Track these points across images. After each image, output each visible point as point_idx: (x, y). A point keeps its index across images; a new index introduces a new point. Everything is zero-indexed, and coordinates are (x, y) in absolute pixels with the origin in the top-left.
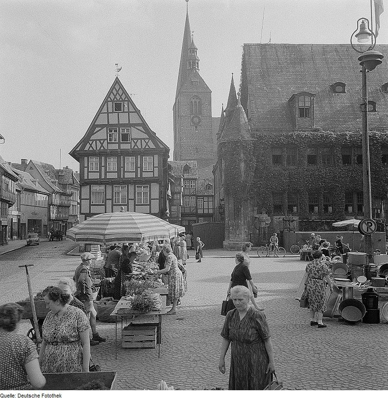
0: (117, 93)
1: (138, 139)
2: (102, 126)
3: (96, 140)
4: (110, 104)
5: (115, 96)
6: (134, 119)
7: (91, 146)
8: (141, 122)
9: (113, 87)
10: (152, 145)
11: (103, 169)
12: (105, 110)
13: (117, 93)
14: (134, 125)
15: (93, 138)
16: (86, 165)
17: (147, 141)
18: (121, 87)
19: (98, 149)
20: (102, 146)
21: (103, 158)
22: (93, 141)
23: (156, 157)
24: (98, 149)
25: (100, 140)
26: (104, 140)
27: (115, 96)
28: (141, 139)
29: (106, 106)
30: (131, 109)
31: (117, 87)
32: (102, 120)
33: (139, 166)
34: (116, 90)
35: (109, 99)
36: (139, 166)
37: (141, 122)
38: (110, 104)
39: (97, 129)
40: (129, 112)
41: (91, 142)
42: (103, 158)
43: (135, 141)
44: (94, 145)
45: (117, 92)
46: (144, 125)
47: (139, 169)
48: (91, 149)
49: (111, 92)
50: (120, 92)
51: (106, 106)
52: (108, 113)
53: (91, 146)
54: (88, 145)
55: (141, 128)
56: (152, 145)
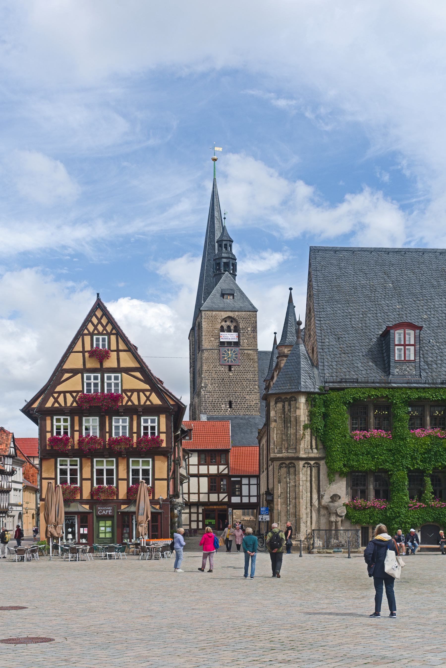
0: (100, 322)
1: (132, 391)
2: (75, 372)
3: (65, 392)
4: (87, 339)
5: (96, 327)
6: (127, 361)
7: (56, 401)
8: (138, 366)
9: (92, 313)
10: (155, 400)
11: (77, 435)
12: (78, 347)
13: (100, 322)
14: (127, 370)
15: (59, 388)
16: (48, 429)
17: (148, 394)
18: (106, 313)
19: (69, 405)
20: (74, 400)
21: (76, 419)
22: (59, 393)
23: (163, 419)
24: (69, 405)
25: (71, 392)
26: (77, 392)
27: (96, 327)
28: (138, 391)
29: (80, 343)
30: (122, 346)
31: (99, 313)
32: (75, 362)
33: (135, 430)
34: (97, 317)
35: (86, 332)
36: (135, 430)
37: (138, 366)
38: (87, 339)
39: (66, 375)
40: (118, 351)
41: (56, 395)
42: (76, 419)
43: (129, 394)
44: (61, 399)
45: (99, 320)
46: (143, 369)
47: (135, 436)
48: (56, 405)
49: (88, 320)
50: (104, 321)
51: (80, 340)
52: (83, 352)
53: (56, 401)
54: (52, 400)
55: (138, 374)
56: (155, 400)
